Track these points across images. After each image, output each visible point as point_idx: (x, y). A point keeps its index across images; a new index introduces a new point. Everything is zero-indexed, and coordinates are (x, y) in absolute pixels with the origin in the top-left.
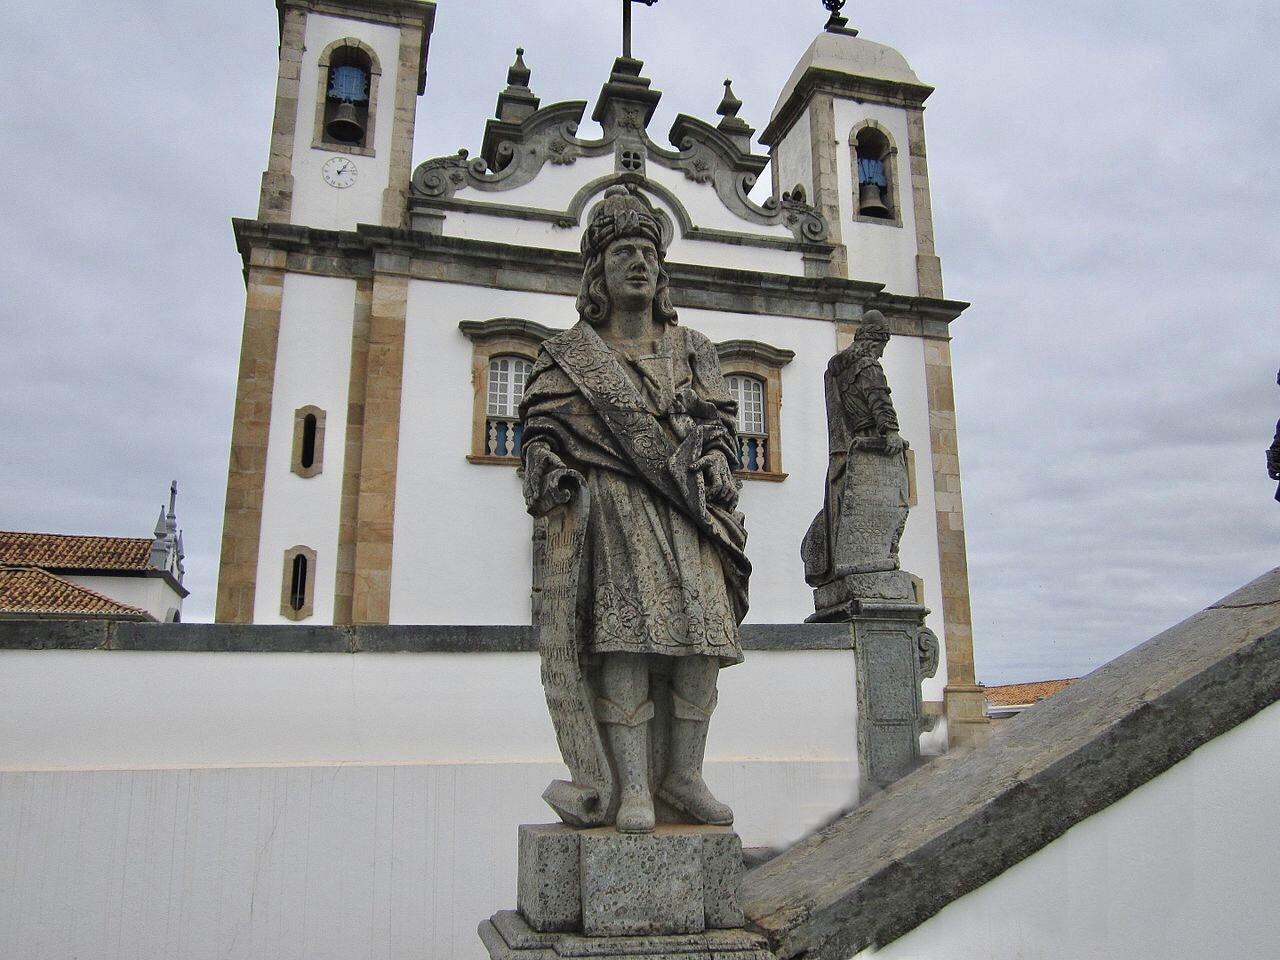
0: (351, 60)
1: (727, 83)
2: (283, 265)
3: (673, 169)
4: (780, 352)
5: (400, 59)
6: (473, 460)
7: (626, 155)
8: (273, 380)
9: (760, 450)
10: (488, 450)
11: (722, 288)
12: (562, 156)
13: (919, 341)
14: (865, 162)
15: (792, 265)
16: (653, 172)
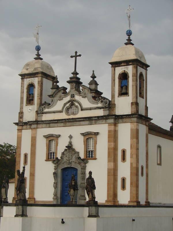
0: (31, 86)
1: (93, 71)
2: (21, 129)
3: (80, 96)
4: (95, 133)
5: (38, 84)
6: (46, 161)
7: (72, 95)
8: (21, 149)
9: (93, 153)
10: (49, 158)
11: (87, 120)
12: (61, 99)
13: (130, 123)
14: (124, 81)
15: (101, 113)
16: (77, 97)
